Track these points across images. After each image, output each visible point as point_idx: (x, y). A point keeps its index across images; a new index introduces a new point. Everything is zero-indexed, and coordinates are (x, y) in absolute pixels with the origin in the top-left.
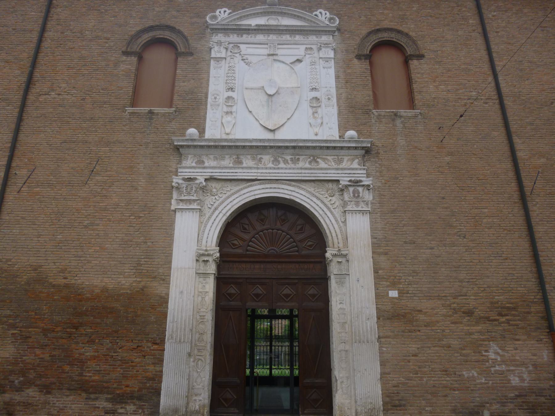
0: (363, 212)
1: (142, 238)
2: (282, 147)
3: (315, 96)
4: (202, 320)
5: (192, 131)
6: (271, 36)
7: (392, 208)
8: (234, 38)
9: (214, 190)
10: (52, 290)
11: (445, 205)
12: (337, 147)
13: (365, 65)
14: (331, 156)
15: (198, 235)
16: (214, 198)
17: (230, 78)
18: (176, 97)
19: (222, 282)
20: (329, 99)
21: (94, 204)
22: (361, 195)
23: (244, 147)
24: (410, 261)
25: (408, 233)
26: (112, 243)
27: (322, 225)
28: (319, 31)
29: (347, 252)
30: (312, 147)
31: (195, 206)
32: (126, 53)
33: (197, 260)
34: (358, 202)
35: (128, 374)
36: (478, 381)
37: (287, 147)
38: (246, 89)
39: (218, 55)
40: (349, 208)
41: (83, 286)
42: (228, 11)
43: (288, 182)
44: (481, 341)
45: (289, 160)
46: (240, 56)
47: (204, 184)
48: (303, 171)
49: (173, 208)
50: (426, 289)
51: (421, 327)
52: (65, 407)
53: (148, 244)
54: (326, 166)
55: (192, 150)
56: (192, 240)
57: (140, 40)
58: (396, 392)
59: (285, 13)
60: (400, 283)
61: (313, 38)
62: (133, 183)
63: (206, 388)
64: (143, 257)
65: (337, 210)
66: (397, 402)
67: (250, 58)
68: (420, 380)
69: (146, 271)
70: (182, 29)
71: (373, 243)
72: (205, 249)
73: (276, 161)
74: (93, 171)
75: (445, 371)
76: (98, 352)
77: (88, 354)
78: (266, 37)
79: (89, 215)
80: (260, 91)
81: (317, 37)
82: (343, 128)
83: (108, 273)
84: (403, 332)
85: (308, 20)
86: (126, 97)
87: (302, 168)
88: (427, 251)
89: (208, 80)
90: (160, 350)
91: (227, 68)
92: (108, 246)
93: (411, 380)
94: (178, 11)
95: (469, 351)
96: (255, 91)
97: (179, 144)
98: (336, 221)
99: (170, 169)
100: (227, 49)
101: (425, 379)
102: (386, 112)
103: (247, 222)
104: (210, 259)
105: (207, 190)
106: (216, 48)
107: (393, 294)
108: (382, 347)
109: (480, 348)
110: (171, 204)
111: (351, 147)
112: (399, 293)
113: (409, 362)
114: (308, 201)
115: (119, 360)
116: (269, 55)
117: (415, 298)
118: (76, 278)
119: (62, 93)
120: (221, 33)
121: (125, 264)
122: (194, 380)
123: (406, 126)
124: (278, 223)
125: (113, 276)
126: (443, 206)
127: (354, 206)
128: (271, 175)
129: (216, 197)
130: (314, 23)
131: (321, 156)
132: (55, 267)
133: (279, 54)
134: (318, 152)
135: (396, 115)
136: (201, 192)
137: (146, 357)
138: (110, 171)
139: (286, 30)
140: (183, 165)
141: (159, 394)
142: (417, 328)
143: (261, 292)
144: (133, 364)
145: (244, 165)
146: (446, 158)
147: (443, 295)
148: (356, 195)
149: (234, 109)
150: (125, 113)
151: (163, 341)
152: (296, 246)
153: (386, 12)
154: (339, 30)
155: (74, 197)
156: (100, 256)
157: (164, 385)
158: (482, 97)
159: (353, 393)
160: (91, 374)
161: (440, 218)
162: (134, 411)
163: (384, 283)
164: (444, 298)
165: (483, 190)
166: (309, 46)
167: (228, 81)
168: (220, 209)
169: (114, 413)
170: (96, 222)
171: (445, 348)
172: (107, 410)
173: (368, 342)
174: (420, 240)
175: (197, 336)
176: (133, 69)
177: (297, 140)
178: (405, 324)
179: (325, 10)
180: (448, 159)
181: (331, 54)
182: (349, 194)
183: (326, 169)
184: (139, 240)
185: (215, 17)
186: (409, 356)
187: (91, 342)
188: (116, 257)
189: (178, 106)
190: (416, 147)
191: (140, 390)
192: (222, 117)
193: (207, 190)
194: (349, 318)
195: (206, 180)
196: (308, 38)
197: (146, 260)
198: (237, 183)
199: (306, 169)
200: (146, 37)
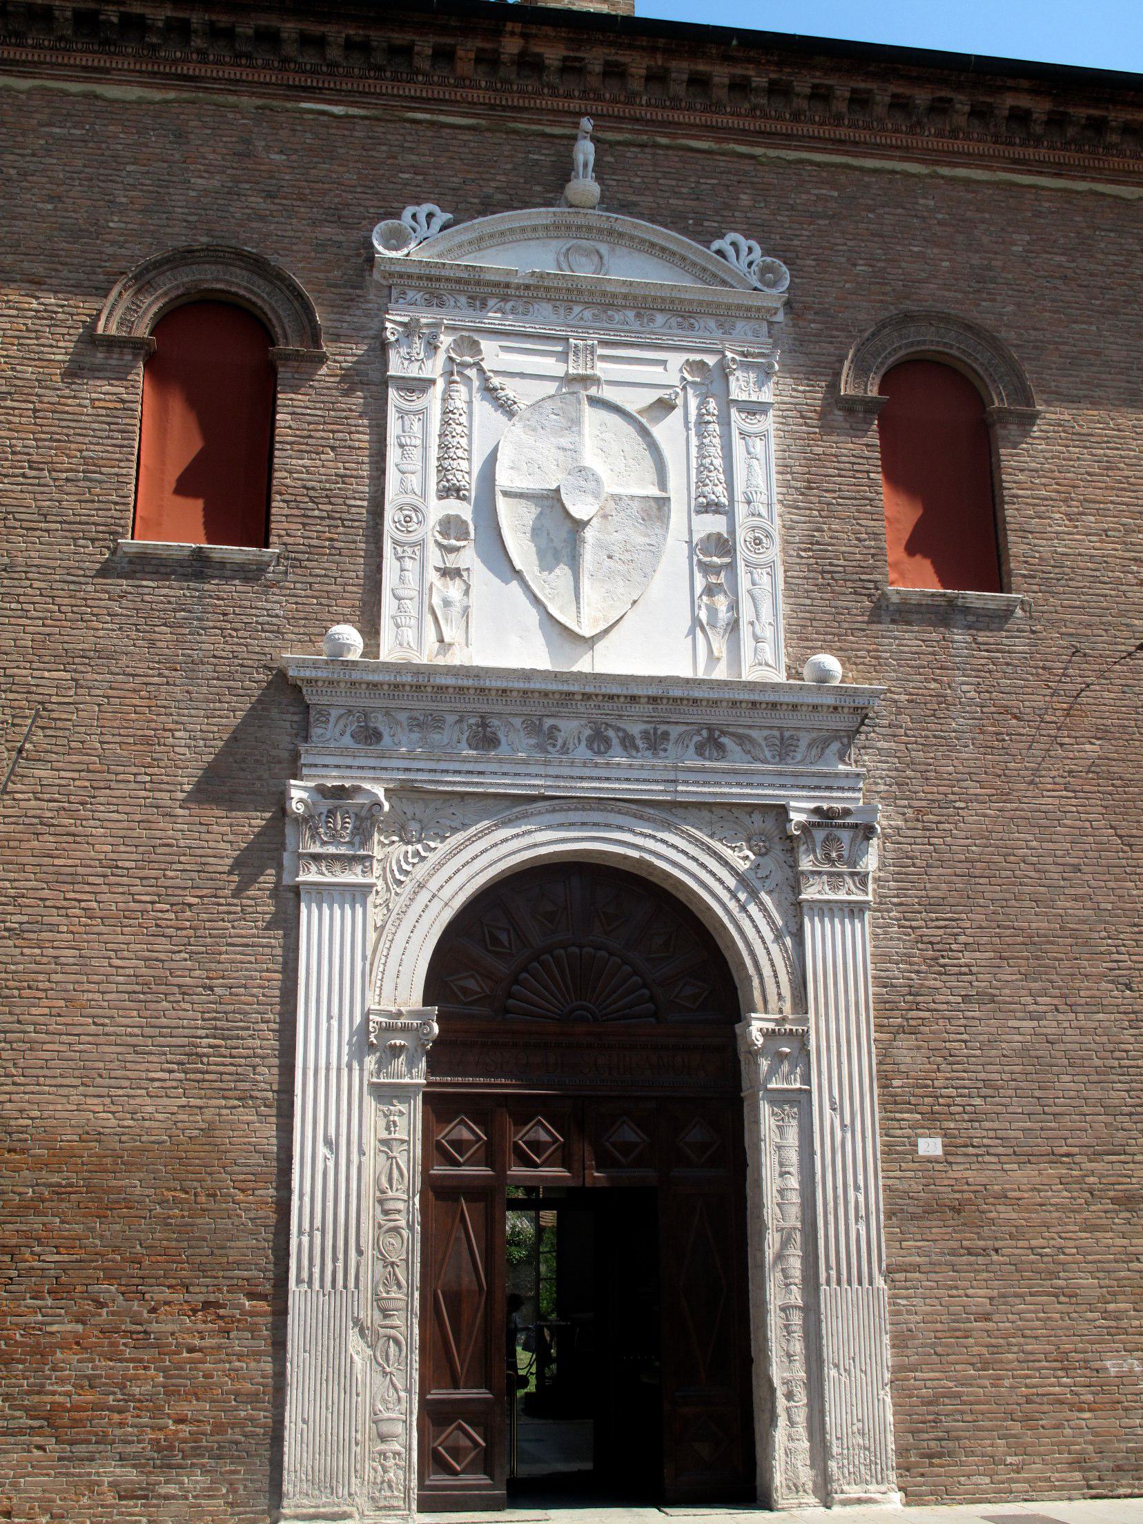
11: (1082, 891)
14: (761, 728)
16: (410, 848)
18: (277, 506)
25: (974, 969)
26: (103, 987)
37: (633, 699)
38: (506, 494)
39: (413, 371)
40: (811, 892)
41: (21, 1122)
43: (634, 807)
45: (638, 736)
58: (931, 1417)
59: (621, 235)
62: (158, 795)
66: (933, 1444)
67: (511, 389)
68: (993, 1385)
72: (394, 1009)
74: (20, 751)
75: (1064, 1363)
76: (84, 1323)
77: (55, 1328)
78: (562, 311)
80: (549, 502)
85: (694, 264)
86: (114, 498)
88: (1025, 1023)
92: (90, 996)
93: (971, 1386)
94: (270, 195)
95: (1122, 1306)
97: (302, 674)
99: (274, 752)
101: (1006, 1382)
107: (930, 1146)
112: (944, 1146)
117: (987, 1158)
120: (418, 289)
123: (980, 639)
125: (113, 1092)
126: (1072, 891)
127: (827, 888)
129: (419, 847)
131: (731, 729)
137: (232, 1335)
138: (79, 752)
139: (625, 297)
146: (1088, 747)
147: (1065, 1149)
152: (652, 999)
153: (932, 252)
160: (69, 1388)
161: (1062, 929)
162: (203, 1489)
163: (906, 1116)
168: (433, 885)
169: (146, 1497)
171: (1062, 1299)
174: (1007, 991)
179: (747, 237)
189: (287, 539)
190: (1006, 710)
191: (219, 1428)
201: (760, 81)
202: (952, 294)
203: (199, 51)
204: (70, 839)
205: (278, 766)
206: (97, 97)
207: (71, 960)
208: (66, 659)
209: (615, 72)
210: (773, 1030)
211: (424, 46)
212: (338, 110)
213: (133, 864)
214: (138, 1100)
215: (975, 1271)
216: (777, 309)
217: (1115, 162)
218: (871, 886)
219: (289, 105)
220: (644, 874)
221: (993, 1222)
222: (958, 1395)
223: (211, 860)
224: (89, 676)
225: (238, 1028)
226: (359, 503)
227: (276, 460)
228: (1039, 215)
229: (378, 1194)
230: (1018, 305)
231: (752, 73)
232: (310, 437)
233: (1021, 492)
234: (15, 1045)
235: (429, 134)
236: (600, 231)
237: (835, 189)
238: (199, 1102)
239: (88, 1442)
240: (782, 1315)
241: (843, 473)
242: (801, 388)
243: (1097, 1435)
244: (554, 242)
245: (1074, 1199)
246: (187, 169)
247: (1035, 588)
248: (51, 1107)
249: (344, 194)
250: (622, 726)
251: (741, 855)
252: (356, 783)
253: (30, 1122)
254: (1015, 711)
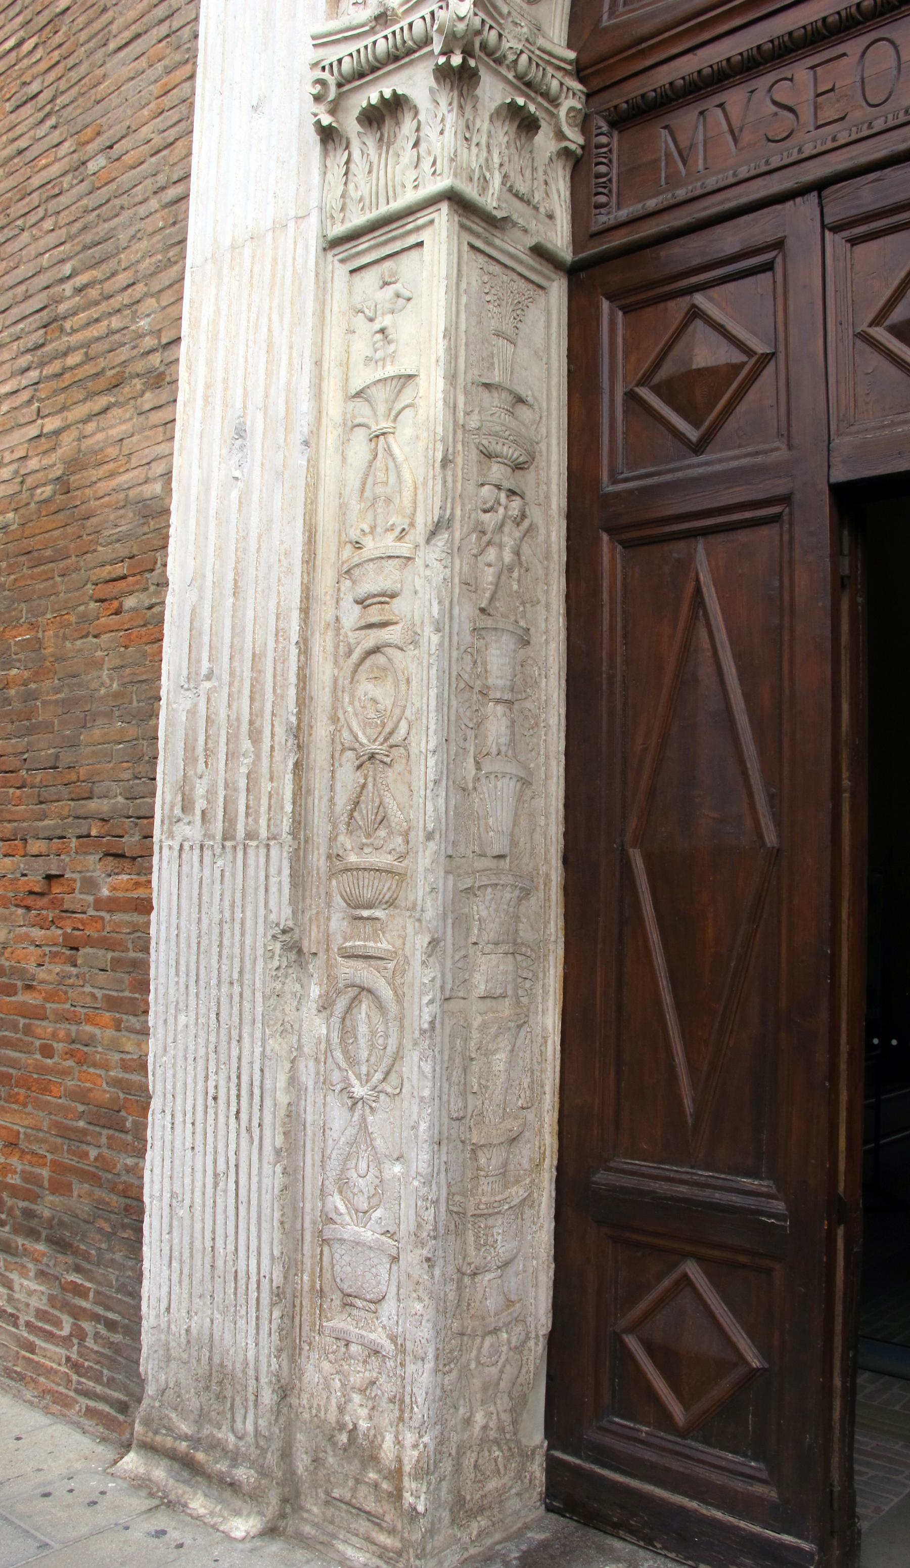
4: (372, 638)
122: (333, 1166)
175: (348, 777)
229: (348, 550)
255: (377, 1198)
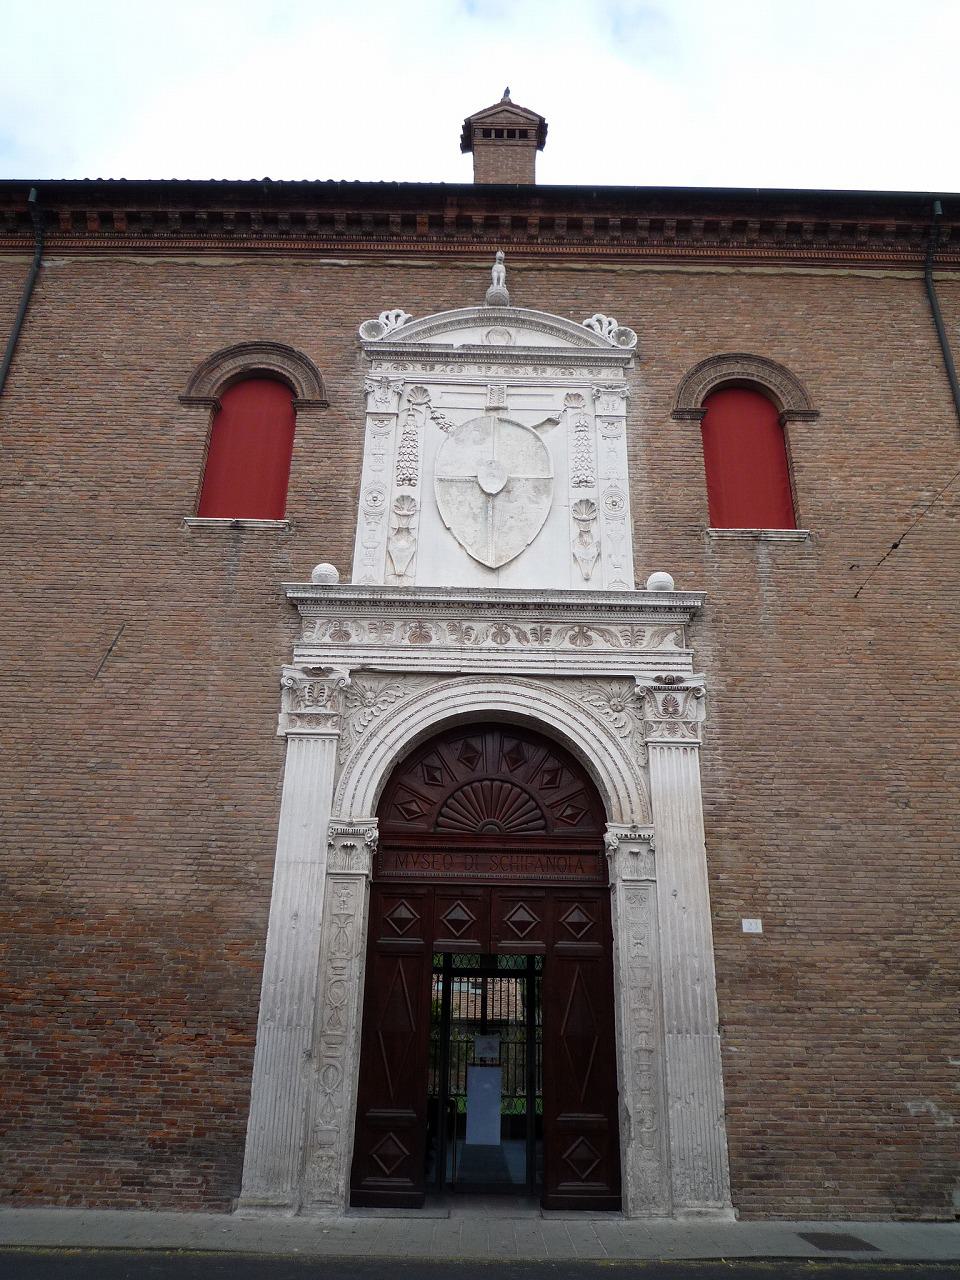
0: (687, 747)
1: (214, 796)
2: (514, 604)
3: (584, 498)
4: (338, 978)
5: (325, 570)
6: (494, 368)
7: (749, 737)
8: (416, 371)
9: (370, 695)
10: (16, 908)
12: (630, 606)
13: (692, 432)
15: (335, 789)
16: (368, 710)
17: (406, 457)
18: (290, 496)
19: (382, 892)
20: (614, 504)
21: (110, 722)
22: (680, 709)
23: (434, 604)
24: (788, 854)
25: (783, 792)
26: (148, 806)
27: (598, 773)
28: (596, 359)
29: (651, 833)
30: (578, 605)
31: (328, 728)
32: (187, 401)
33: (330, 845)
34: (675, 723)
35: (177, 1097)
36: (939, 1124)
37: (524, 606)
38: (441, 480)
40: (654, 737)
41: (82, 900)
42: (405, 316)
43: (525, 679)
44: (946, 1034)
46: (429, 411)
47: (349, 681)
48: (559, 657)
49: (281, 732)
50: (824, 917)
51: (814, 1000)
52: (37, 1169)
53: (226, 808)
54: (606, 646)
55: (323, 610)
56: (323, 798)
57: (217, 374)
59: (524, 321)
60: (767, 903)
61: (582, 375)
63: (344, 1131)
64: (213, 837)
65: (629, 739)
66: (761, 1168)
67: (450, 416)
69: (219, 869)
70: (303, 350)
71: (707, 814)
72: (347, 820)
73: (501, 635)
74: (110, 650)
77: (88, 1051)
78: (483, 369)
79: (101, 745)
81: (591, 373)
82: (645, 563)
83: (139, 872)
84: (774, 1011)
85: (572, 336)
87: (558, 650)
88: (825, 832)
89: (360, 460)
90: (246, 1044)
91: (400, 437)
92: (136, 812)
93: (792, 1119)
94: (299, 313)
96: (459, 484)
97: (296, 595)
98: (628, 763)
99: (276, 648)
100: (400, 395)
102: (736, 532)
103: (437, 763)
104: (359, 844)
105: (354, 695)
106: (378, 393)
107: (752, 926)
108: (729, 1044)
109: (943, 1050)
110: (277, 724)
111: (660, 607)
113: (789, 1079)
114: (569, 721)
115: (155, 1066)
116: (489, 409)
117: (799, 936)
118: (68, 882)
119: (50, 483)
120: (391, 361)
121: (175, 851)
123: (779, 562)
124: (504, 768)
125: (147, 879)
126: (858, 735)
127: (666, 733)
128: (489, 664)
129: (373, 709)
130: (586, 342)
132: (22, 857)
133: (510, 407)
134: (586, 617)
135: (756, 538)
136: (341, 698)
138: (147, 651)
140: (306, 640)
141: (242, 1143)
142: (804, 1003)
143: (466, 918)
144: (186, 1075)
145: (434, 642)
146: (865, 632)
147: (861, 930)
148: (670, 708)
149: (413, 523)
150: (183, 527)
151: (252, 1023)
152: (543, 817)
153: (738, 319)
154: (637, 356)
155: (68, 706)
156: (122, 835)
157: (251, 1123)
158: (943, 503)
159: (664, 1147)
160: (94, 1096)
161: (852, 762)
162: (185, 1180)
164: (862, 938)
165: (947, 702)
166: (575, 391)
167: (402, 464)
168: (381, 735)
169: (142, 1184)
170: (114, 761)
171: (868, 1050)
172: (127, 1178)
173: (697, 1033)
175: (328, 1012)
176: (202, 433)
177: (546, 591)
178: (779, 993)
180: (869, 633)
181: (621, 408)
182: (656, 707)
183: (606, 653)
184: (206, 801)
185: (375, 328)
186: (788, 1065)
187: (96, 1023)
188: (156, 836)
190: (799, 609)
191: (200, 1133)
192: (389, 539)
193: (354, 695)
194: (656, 976)
195: (352, 673)
196: (571, 374)
197: (219, 843)
198: (417, 681)
199: (564, 652)
200: (230, 367)
201: (615, 221)
202: (753, 344)
203: (256, 233)
204: (136, 707)
205: (280, 658)
206: (196, 265)
207: (128, 788)
208: (143, 593)
209: (519, 224)
210: (626, 836)
211: (395, 217)
212: (344, 262)
213: (175, 723)
214: (163, 886)
215: (792, 1026)
216: (629, 359)
217: (866, 255)
218: (700, 733)
219: (313, 261)
220: (537, 729)
221: (804, 987)
222: (783, 1126)
223: (228, 720)
224: (159, 603)
225: (236, 834)
226: (344, 491)
227: (292, 467)
228: (815, 292)
230: (801, 347)
231: (609, 216)
232: (314, 452)
233: (806, 464)
234: (83, 847)
235: (402, 272)
236: (510, 319)
237: (668, 286)
238: (206, 887)
239: (102, 1138)
240: (636, 1056)
241: (676, 458)
242: (647, 407)
243: (901, 1164)
244: (479, 329)
245: (873, 969)
246: (248, 302)
247: (819, 526)
248: (103, 890)
249: (346, 310)
250: (517, 625)
251: (604, 711)
252: (328, 666)
253: (87, 900)
254: (808, 609)
255: (333, 1116)
